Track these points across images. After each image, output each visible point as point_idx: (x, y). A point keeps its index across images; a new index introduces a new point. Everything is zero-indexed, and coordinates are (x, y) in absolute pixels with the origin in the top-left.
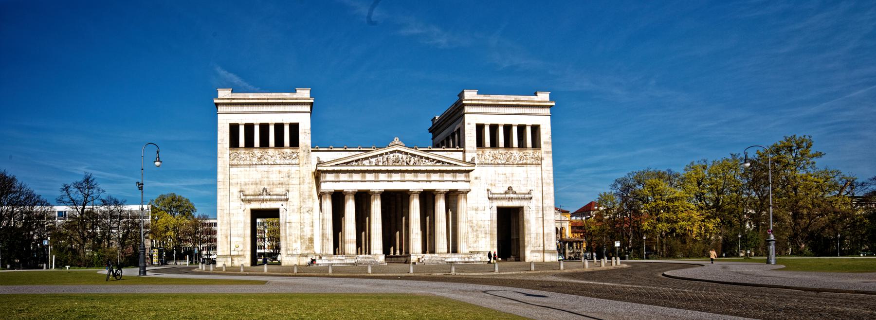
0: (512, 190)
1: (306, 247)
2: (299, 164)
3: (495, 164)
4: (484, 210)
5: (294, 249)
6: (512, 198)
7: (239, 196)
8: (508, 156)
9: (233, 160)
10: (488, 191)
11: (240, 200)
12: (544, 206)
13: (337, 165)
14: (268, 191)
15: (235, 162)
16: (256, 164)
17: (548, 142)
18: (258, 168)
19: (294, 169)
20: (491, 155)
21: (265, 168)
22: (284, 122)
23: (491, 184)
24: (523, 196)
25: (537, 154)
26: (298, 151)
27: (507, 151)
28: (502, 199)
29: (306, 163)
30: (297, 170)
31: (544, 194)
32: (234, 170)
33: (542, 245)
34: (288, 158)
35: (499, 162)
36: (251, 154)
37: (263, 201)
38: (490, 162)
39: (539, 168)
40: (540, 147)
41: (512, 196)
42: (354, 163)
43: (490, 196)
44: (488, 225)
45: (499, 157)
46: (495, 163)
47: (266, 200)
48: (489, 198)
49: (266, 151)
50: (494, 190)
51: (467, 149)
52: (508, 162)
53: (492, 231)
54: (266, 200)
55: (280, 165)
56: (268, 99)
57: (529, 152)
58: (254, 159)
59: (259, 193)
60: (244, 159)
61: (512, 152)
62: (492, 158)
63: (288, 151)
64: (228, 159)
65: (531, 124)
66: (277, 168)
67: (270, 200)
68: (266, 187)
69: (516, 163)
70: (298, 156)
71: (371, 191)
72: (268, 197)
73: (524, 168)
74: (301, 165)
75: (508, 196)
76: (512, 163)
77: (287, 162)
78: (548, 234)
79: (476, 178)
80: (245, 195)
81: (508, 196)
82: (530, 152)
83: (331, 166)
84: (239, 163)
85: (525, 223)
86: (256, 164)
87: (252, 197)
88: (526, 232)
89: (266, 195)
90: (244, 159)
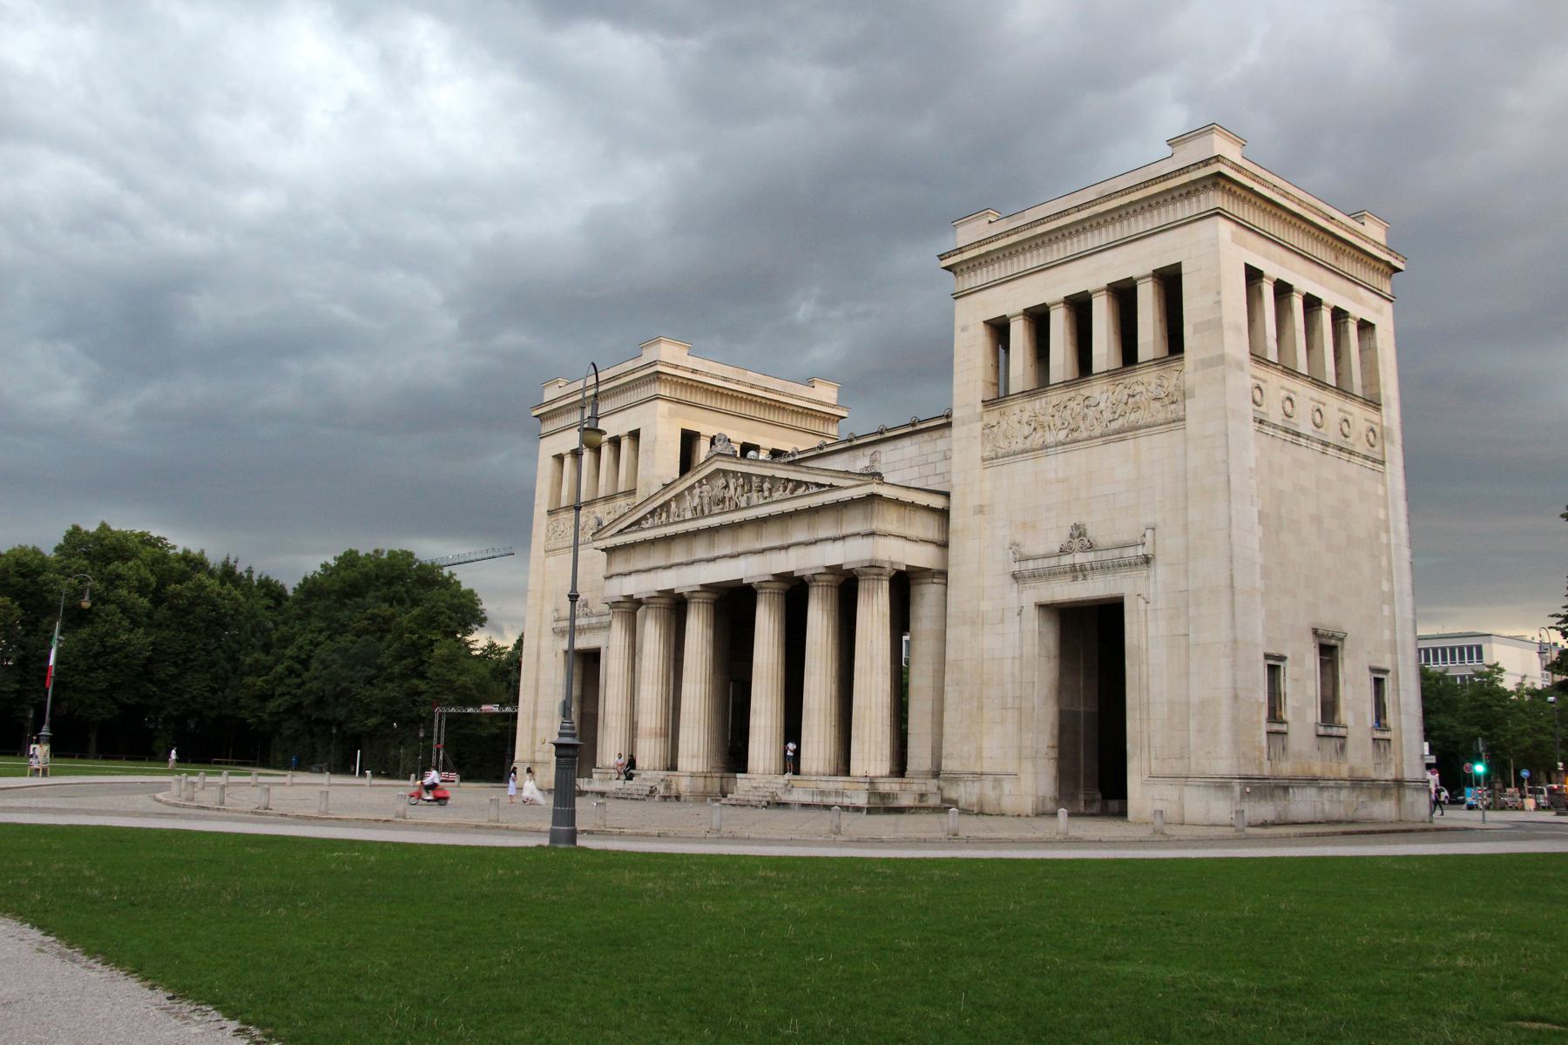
3: (1034, 450)
4: (1002, 621)
6: (1083, 569)
8: (1078, 409)
13: (621, 532)
14: (590, 605)
24: (1116, 553)
25: (1170, 378)
27: (1073, 394)
28: (1051, 574)
35: (1050, 438)
38: (1020, 446)
39: (1178, 435)
41: (1080, 558)
42: (650, 521)
43: (1016, 567)
45: (1046, 419)
50: (1029, 549)
52: (1075, 435)
62: (1027, 430)
65: (1150, 271)
69: (1097, 432)
73: (1129, 446)
75: (1067, 560)
76: (1085, 435)
79: (980, 510)
81: (1067, 560)
84: (557, 547)
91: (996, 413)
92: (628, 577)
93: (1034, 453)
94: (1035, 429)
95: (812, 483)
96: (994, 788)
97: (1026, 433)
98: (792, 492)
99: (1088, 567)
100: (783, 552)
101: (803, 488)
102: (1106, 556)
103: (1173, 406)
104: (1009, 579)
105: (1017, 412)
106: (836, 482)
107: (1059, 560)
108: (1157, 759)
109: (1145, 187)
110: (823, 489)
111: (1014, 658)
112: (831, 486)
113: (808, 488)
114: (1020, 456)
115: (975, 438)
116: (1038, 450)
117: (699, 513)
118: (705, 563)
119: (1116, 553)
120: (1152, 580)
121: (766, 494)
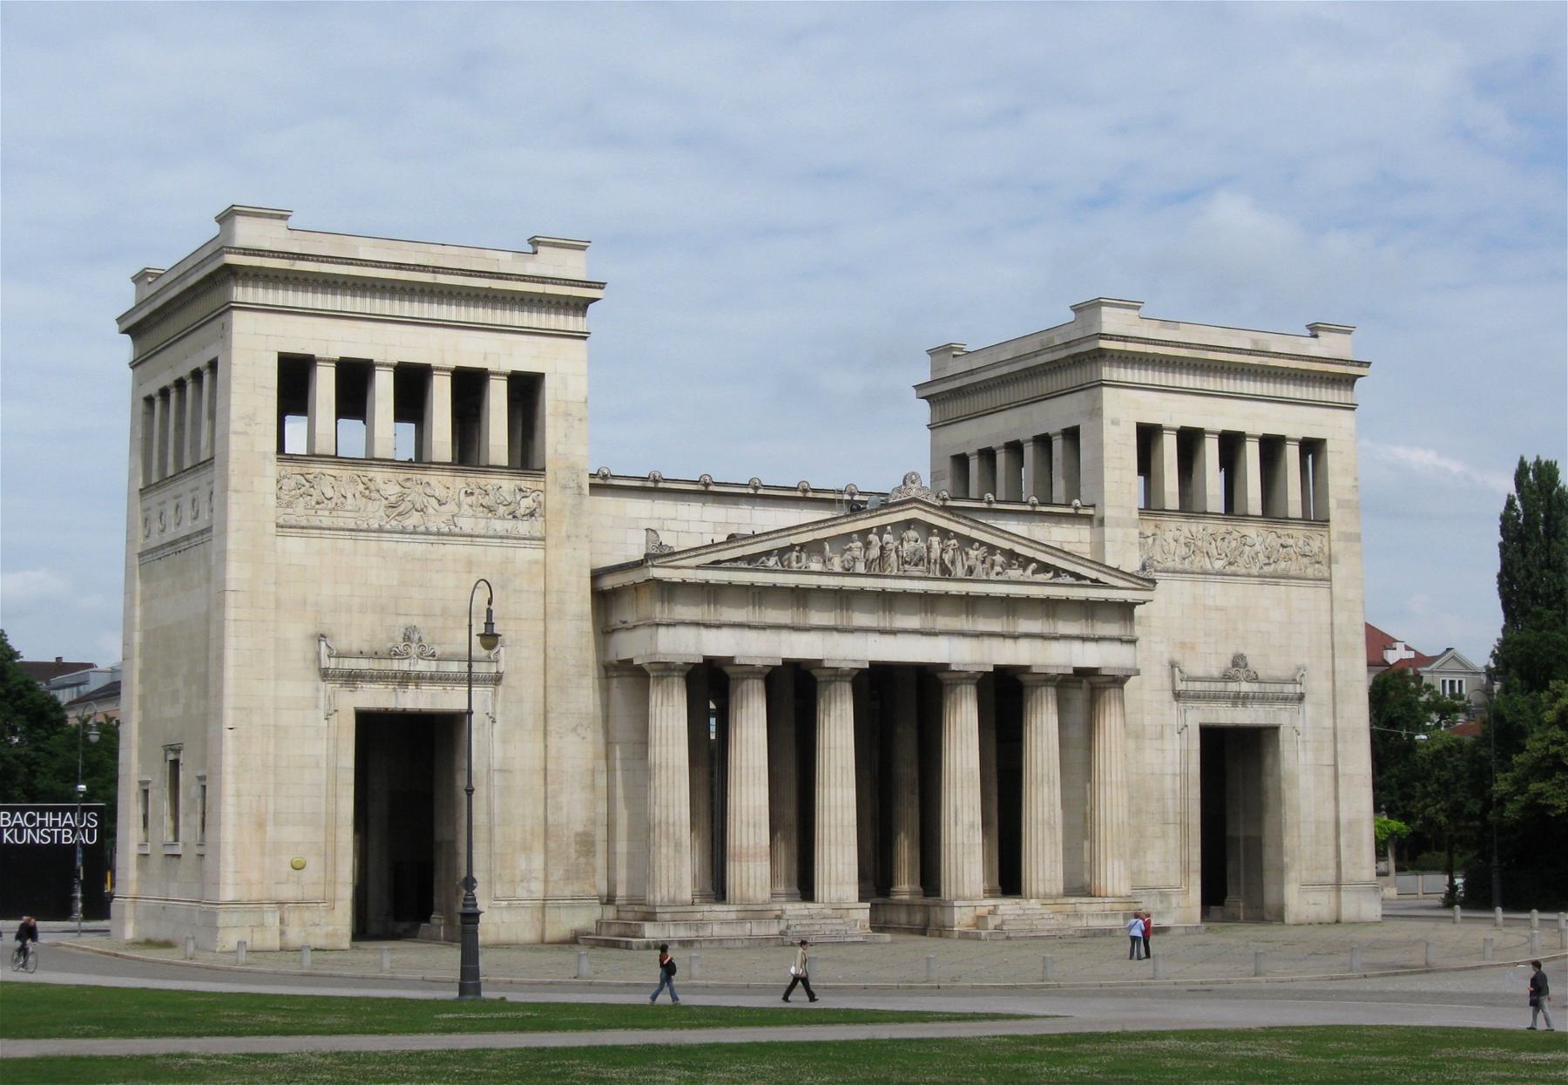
0: (1246, 665)
1: (567, 871)
2: (543, 539)
4: (1161, 736)
5: (518, 878)
7: (311, 655)
8: (1234, 544)
9: (289, 505)
10: (1173, 665)
11: (313, 674)
12: (1339, 726)
13: (716, 564)
15: (298, 514)
16: (381, 530)
17: (1349, 501)
18: (385, 545)
19: (526, 555)
20: (1182, 540)
21: (418, 548)
22: (491, 367)
23: (1183, 645)
24: (1277, 688)
26: (541, 486)
27: (1230, 528)
28: (1215, 697)
29: (569, 537)
30: (536, 562)
31: (1337, 683)
32: (294, 545)
33: (1332, 864)
34: (501, 510)
36: (361, 487)
37: (405, 679)
38: (1179, 567)
39: (1323, 593)
40: (1324, 522)
41: (1245, 687)
42: (772, 562)
43: (1181, 686)
44: (1174, 791)
46: (1196, 567)
47: (420, 679)
48: (1177, 696)
49: (417, 475)
51: (1109, 513)
53: (1185, 813)
54: (420, 679)
55: (471, 536)
56: (436, 270)
57: (1295, 533)
58: (371, 506)
59: (390, 645)
60: (331, 505)
61: (1245, 531)
62: (1184, 551)
63: (507, 485)
64: (272, 501)
66: (456, 550)
67: (433, 679)
68: (416, 621)
69: (1255, 571)
70: (540, 503)
71: (827, 664)
72: (423, 666)
74: (550, 542)
75: (1233, 687)
76: (1243, 571)
77: (499, 526)
78: (1350, 823)
80: (339, 656)
81: (1233, 687)
82: (1297, 535)
83: (698, 567)
85: (1285, 786)
86: (381, 530)
87: (364, 664)
88: (1289, 816)
89: (421, 656)
90: (331, 505)
91: (1152, 524)
92: (713, 633)
93: (1192, 576)
94: (1193, 552)
95: (1065, 571)
96: (1161, 902)
97: (1183, 553)
98: (1034, 573)
99: (1251, 695)
100: (1009, 643)
101: (1051, 574)
102: (1271, 688)
103: (1317, 566)
104: (1168, 695)
105: (1174, 529)
106: (1103, 578)
107: (1226, 685)
108: (1307, 869)
109: (1310, 361)
110: (1084, 582)
111: (1175, 775)
112: (1096, 583)
113: (1054, 577)
114: (1179, 575)
115: (1132, 544)
116: (1198, 574)
117: (877, 567)
118: (878, 635)
119: (1277, 688)
120: (1301, 715)
121: (998, 569)
